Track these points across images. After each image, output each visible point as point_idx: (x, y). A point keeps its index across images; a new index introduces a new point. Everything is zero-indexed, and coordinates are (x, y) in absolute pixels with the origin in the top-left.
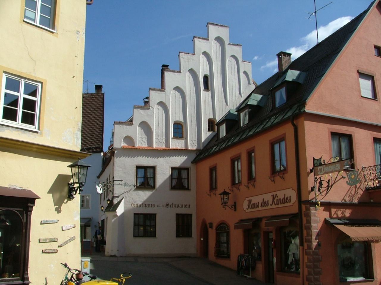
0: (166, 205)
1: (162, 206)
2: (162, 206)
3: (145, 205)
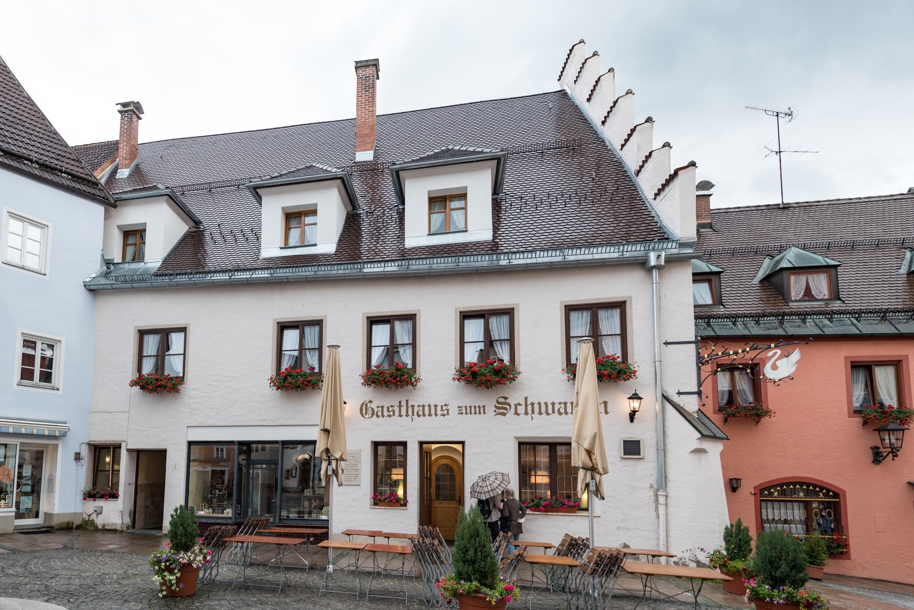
0: (496, 407)
3: (410, 409)
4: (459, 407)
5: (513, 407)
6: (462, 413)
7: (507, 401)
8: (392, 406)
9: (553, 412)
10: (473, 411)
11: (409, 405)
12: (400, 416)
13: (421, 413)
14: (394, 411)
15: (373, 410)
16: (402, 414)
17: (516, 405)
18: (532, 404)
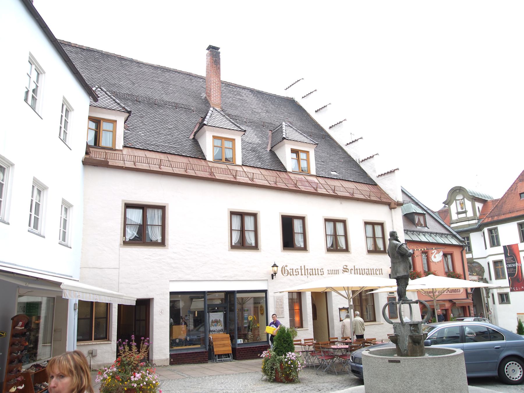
0: (343, 270)
3: (306, 271)
4: (328, 270)
5: (350, 270)
6: (329, 274)
8: (297, 269)
9: (365, 274)
11: (306, 269)
12: (302, 275)
13: (311, 273)
14: (298, 272)
15: (288, 271)
16: (303, 274)
17: (351, 270)
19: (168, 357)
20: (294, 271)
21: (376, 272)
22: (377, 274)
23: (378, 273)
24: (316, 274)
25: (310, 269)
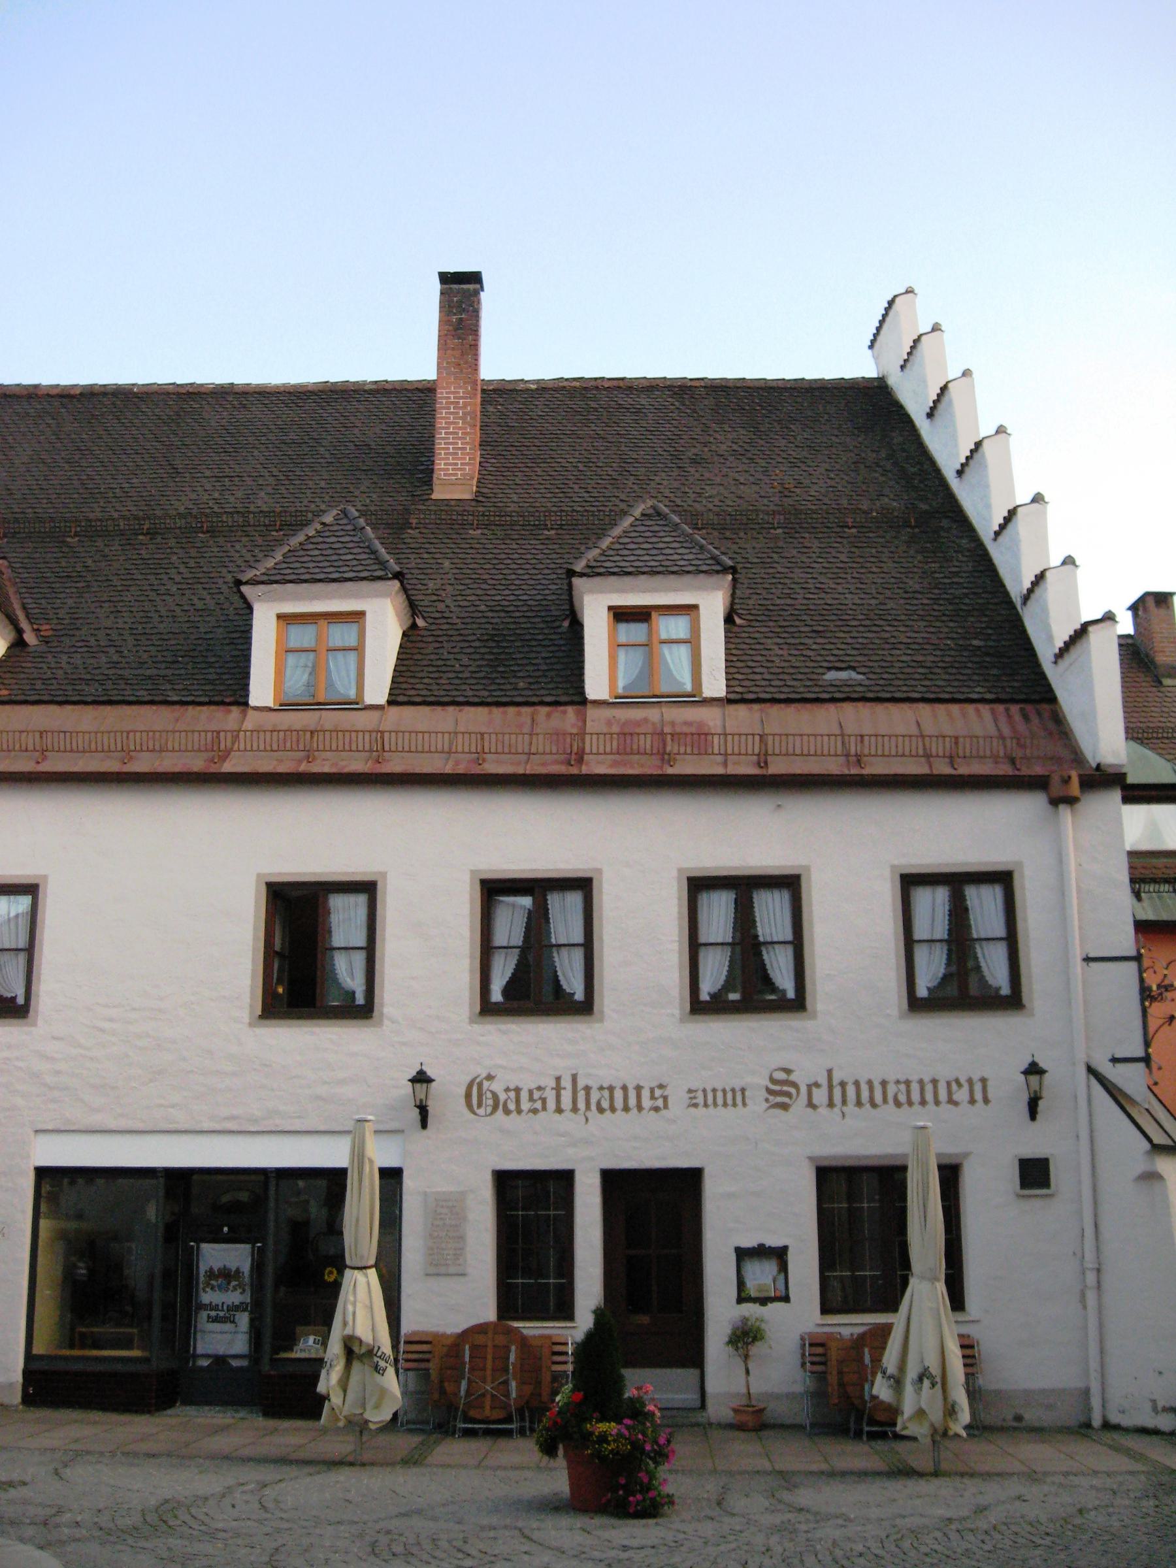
0: (770, 1091)
1: (736, 1097)
2: (736, 1097)
3: (581, 1095)
4: (690, 1091)
5: (803, 1089)
6: (695, 1105)
7: (793, 1077)
8: (539, 1088)
9: (885, 1100)
10: (720, 1101)
12: (559, 1110)
13: (605, 1104)
14: (544, 1101)
15: (495, 1097)
16: (563, 1106)
17: (809, 1086)
18: (587, 1089)
19: (18, 1377)
20: (524, 1095)
21: (950, 1093)
22: (956, 1104)
23: (962, 1095)
24: (626, 1109)
25: (601, 1088)
